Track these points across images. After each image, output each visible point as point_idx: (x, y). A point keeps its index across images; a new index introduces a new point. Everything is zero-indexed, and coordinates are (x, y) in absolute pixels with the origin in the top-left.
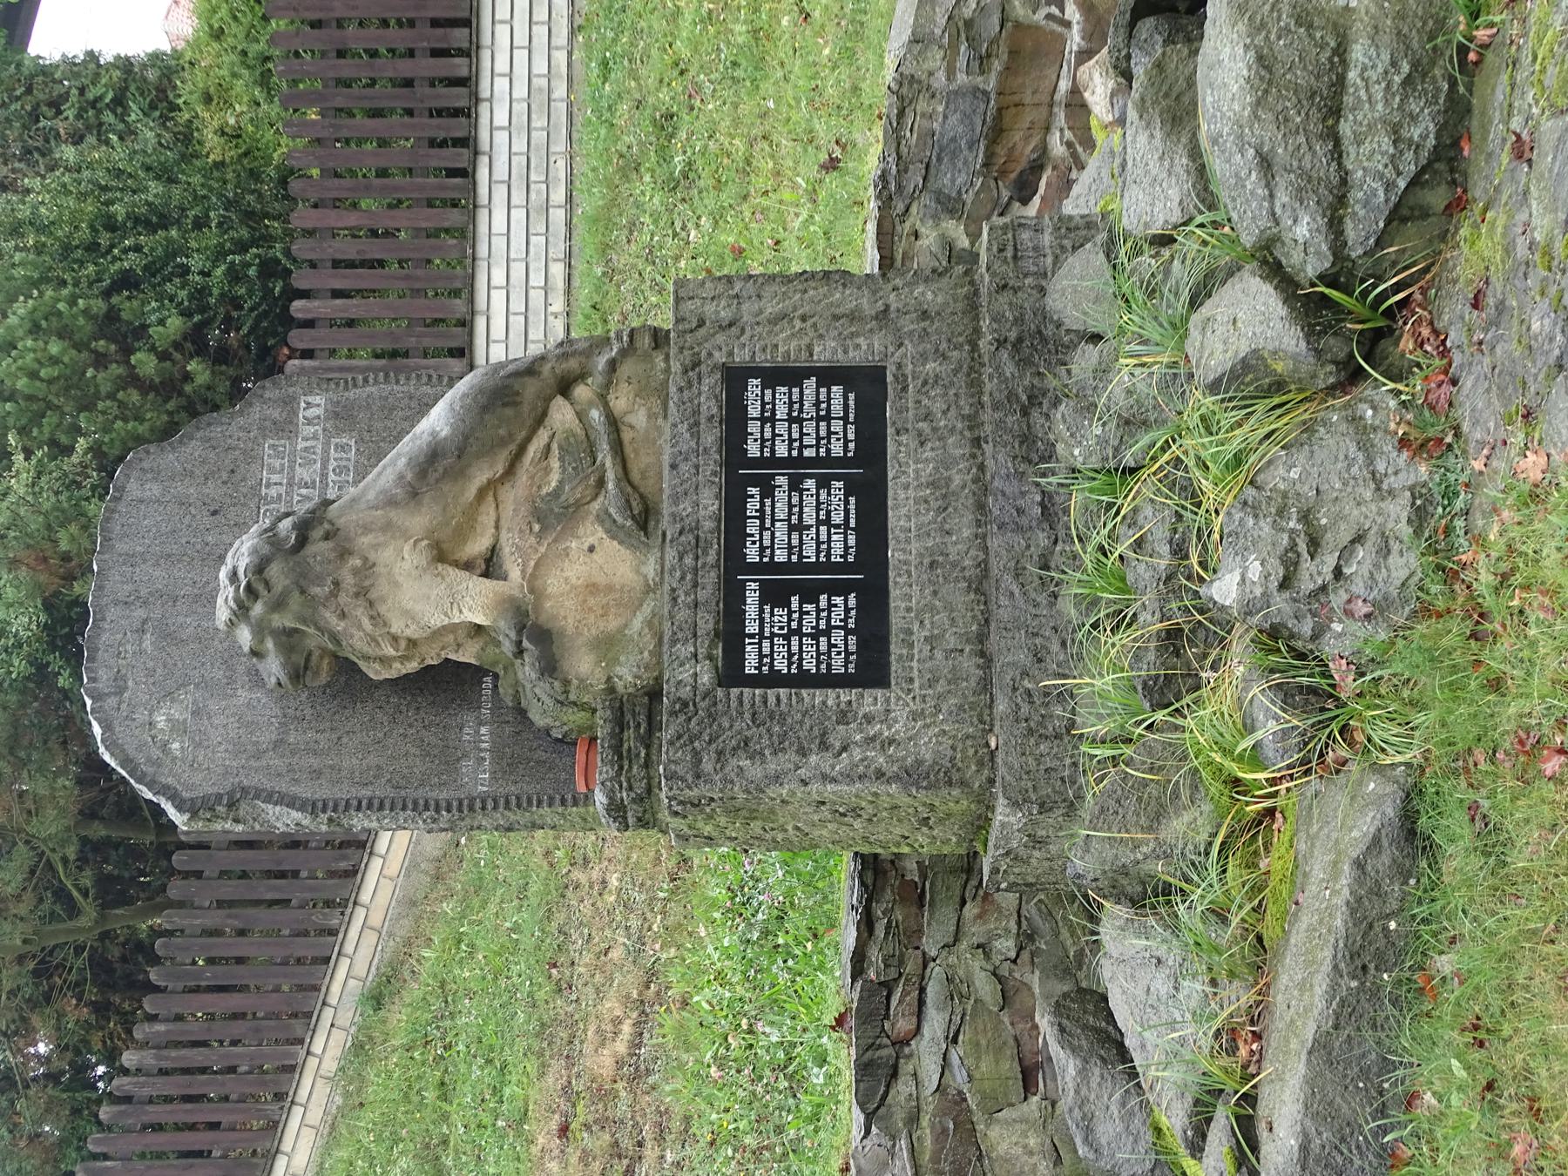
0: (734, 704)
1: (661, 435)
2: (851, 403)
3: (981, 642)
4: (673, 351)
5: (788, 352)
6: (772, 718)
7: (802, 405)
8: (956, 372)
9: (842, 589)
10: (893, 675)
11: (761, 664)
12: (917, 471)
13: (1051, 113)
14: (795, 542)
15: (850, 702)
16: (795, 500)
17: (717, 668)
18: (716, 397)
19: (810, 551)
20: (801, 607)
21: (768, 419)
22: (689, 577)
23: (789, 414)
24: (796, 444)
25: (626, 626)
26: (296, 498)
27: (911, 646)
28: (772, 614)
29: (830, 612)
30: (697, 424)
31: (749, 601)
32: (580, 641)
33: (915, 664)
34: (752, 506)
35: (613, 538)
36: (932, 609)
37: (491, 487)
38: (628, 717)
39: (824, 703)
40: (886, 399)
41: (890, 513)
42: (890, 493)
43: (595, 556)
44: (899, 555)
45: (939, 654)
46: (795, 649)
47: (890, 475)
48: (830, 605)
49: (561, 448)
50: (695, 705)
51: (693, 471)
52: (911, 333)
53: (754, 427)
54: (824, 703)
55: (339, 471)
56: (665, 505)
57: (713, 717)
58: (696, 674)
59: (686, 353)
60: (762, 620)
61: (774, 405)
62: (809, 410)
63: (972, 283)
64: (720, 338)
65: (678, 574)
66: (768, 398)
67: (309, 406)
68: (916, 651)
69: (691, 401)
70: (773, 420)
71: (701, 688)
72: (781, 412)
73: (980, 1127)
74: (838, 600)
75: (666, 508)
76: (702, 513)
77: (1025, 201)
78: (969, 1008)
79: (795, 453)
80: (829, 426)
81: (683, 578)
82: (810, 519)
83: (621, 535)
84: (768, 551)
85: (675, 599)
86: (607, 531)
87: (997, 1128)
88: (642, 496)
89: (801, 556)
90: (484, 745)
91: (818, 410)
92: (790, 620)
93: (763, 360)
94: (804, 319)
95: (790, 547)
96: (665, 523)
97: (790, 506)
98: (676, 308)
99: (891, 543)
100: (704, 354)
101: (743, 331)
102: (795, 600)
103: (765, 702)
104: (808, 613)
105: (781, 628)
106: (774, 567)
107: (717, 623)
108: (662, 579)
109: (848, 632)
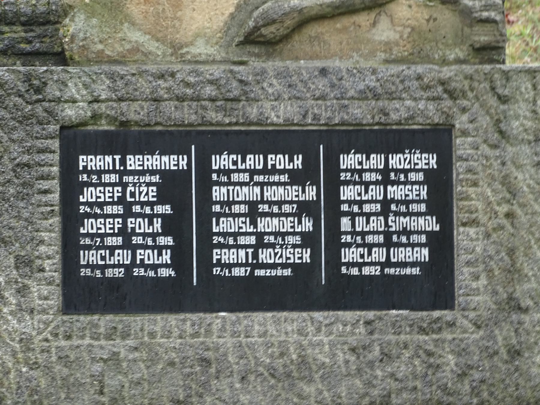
0: (39, 144)
1: (366, 58)
2: (408, 271)
4: (468, 69)
5: (468, 198)
6: (24, 185)
7: (405, 215)
8: (444, 389)
10: (75, 317)
11: (90, 173)
12: (320, 344)
14: (236, 209)
15: (42, 270)
16: (287, 208)
17: (84, 124)
18: (412, 117)
20: (158, 216)
22: (189, 91)
23: (393, 200)
24: (356, 209)
25: (133, 24)
27: (109, 337)
28: (148, 185)
29: (153, 248)
30: (377, 97)
31: (165, 159)
33: (87, 341)
36: (153, 360)
38: (39, 30)
39: (42, 242)
40: (413, 309)
41: (269, 315)
42: (295, 315)
45: (97, 367)
46: (108, 210)
47: (318, 315)
48: (160, 249)
50: (38, 101)
51: (318, 93)
52: (491, 337)
54: (42, 242)
56: (278, 64)
57: (25, 120)
58: (74, 101)
59: (466, 83)
61: (405, 183)
64: (485, 121)
65: (192, 79)
66: (412, 176)
68: (103, 342)
69: (406, 90)
70: (386, 182)
71: (58, 108)
74: (167, 257)
76: (268, 105)
79: (345, 208)
80: (378, 245)
81: (188, 85)
82: (263, 225)
83: (242, 16)
85: (162, 76)
88: (286, 38)
89: (219, 215)
91: (399, 233)
92: (143, 204)
93: (459, 167)
94: (509, 215)
95: (229, 203)
96: (256, 64)
97: (280, 203)
98: (520, 71)
99: (232, 316)
100: (465, 103)
101: (495, 147)
102: (167, 209)
103: (42, 178)
104: (151, 223)
105: (133, 195)
107: (137, 123)
108: (190, 62)
109: (128, 268)
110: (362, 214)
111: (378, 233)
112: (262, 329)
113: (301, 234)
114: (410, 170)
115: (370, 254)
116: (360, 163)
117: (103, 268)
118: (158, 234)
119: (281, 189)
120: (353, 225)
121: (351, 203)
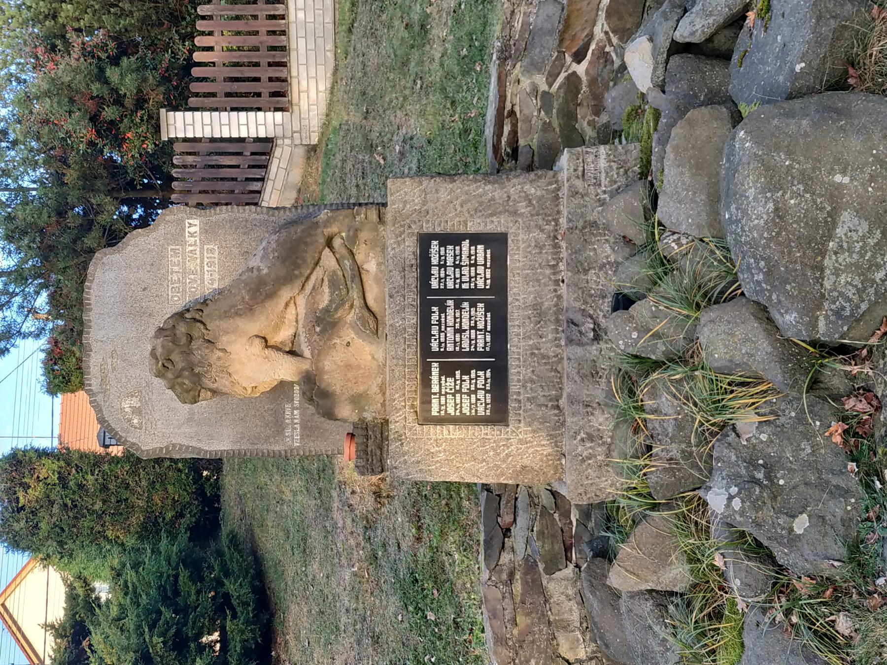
2: (489, 256)
3: (558, 401)
7: (461, 257)
9: (482, 367)
11: (440, 410)
13: (597, 15)
14: (458, 339)
19: (466, 345)
20: (461, 378)
21: (443, 266)
23: (454, 263)
24: (458, 281)
26: (188, 281)
28: (446, 381)
29: (476, 380)
31: (433, 373)
32: (343, 398)
34: (435, 318)
35: (360, 337)
37: (293, 299)
43: (350, 348)
44: (514, 349)
46: (458, 401)
47: (510, 299)
48: (477, 376)
49: (329, 281)
53: (435, 271)
55: (210, 264)
60: (440, 385)
61: (446, 257)
62: (465, 261)
63: (557, 182)
66: (442, 253)
67: (191, 225)
68: (522, 405)
70: (445, 266)
72: (450, 262)
73: (545, 583)
74: (481, 373)
75: (388, 322)
77: (579, 62)
78: (539, 511)
79: (457, 286)
80: (476, 270)
84: (443, 345)
86: (356, 334)
87: (553, 584)
89: (461, 348)
90: (296, 421)
91: (470, 260)
92: (455, 385)
93: (438, 230)
95: (455, 343)
97: (455, 318)
102: (458, 373)
104: (465, 381)
106: (446, 354)
109: (487, 392)
110: (461, 278)
111: (470, 270)
112: (516, 327)
113: (470, 308)
114: (439, 254)
115: (480, 274)
116: (436, 278)
117: (486, 404)
118: (470, 377)
119: (448, 317)
120: (466, 282)
121: (455, 284)
